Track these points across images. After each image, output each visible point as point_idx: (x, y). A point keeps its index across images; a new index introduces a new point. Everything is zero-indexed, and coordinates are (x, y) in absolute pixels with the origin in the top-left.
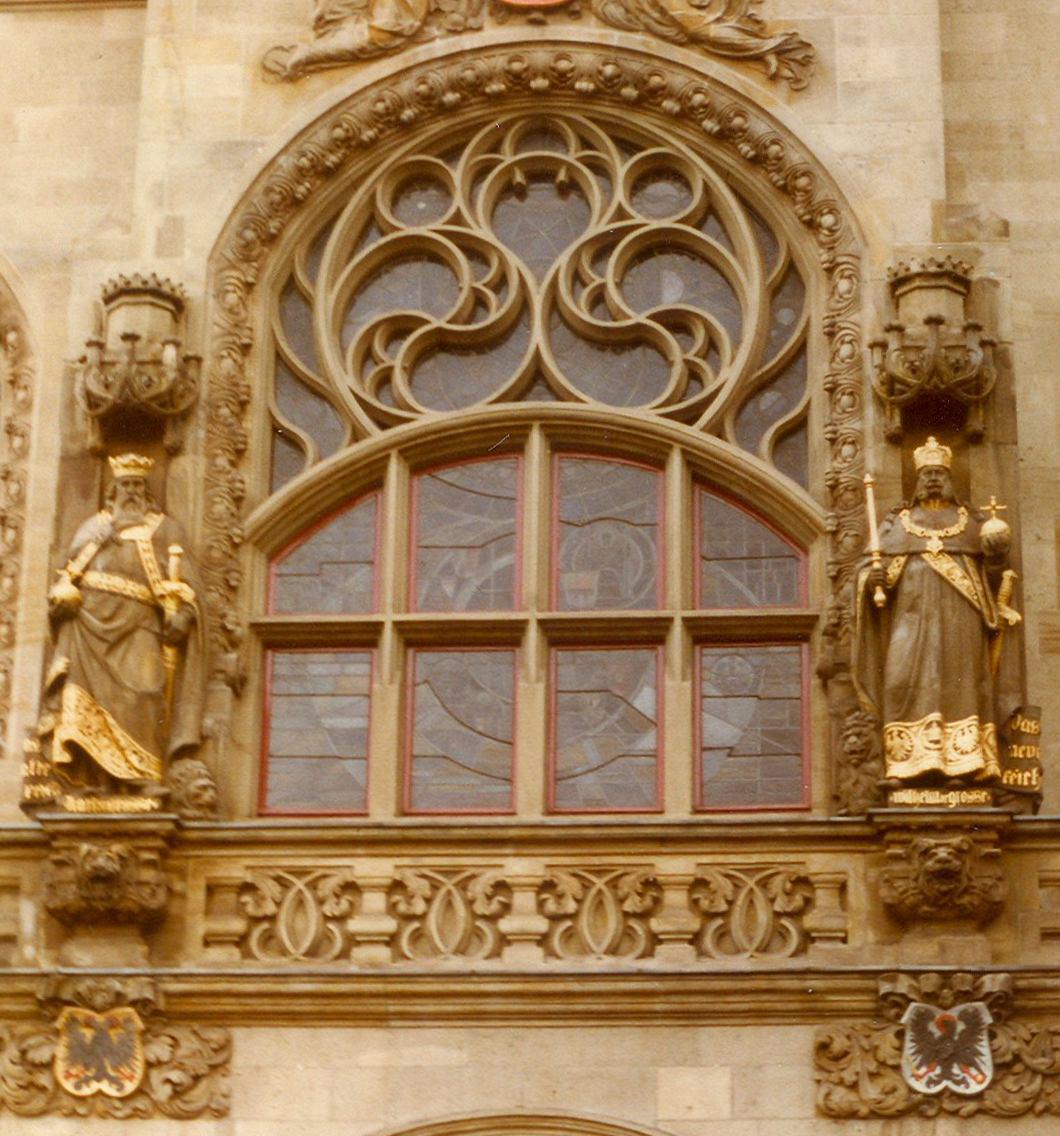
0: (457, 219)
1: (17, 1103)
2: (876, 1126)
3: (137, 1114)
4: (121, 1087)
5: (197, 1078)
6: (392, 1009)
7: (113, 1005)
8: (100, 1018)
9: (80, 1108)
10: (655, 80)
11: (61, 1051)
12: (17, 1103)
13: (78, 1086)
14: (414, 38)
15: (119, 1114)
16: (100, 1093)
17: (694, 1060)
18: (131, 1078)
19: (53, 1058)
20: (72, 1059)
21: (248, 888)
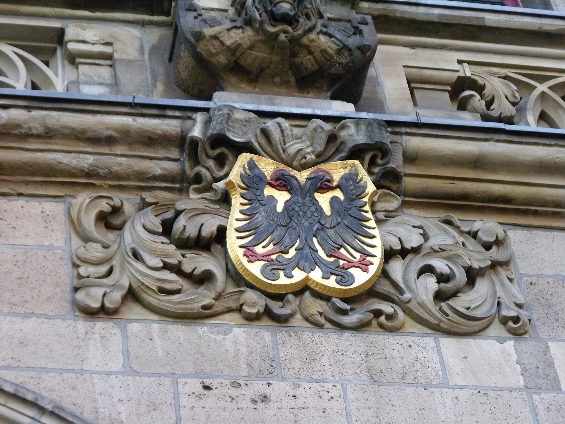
1: (162, 291)
4: (344, 277)
9: (274, 309)
12: (162, 291)
13: (273, 267)
15: (347, 320)
18: (364, 266)
19: (222, 232)
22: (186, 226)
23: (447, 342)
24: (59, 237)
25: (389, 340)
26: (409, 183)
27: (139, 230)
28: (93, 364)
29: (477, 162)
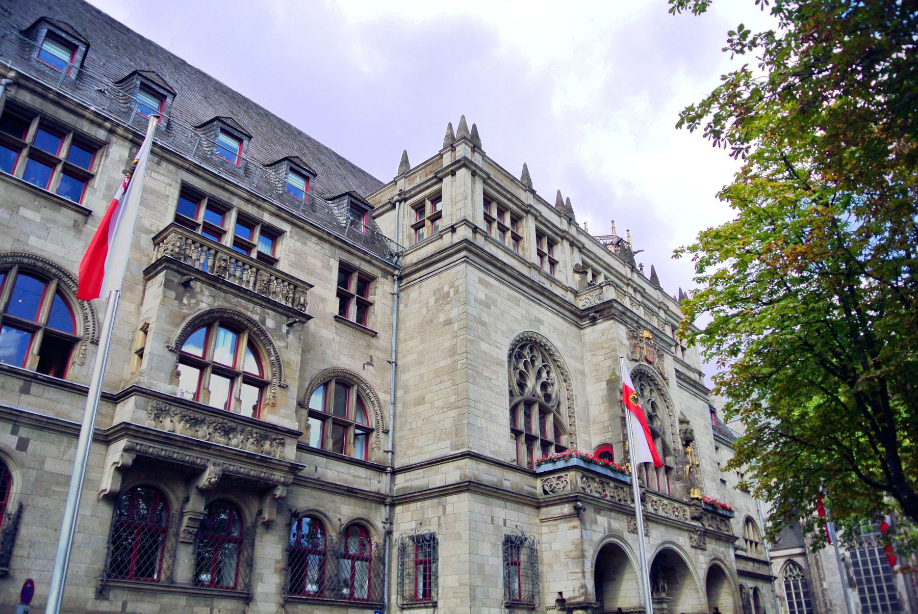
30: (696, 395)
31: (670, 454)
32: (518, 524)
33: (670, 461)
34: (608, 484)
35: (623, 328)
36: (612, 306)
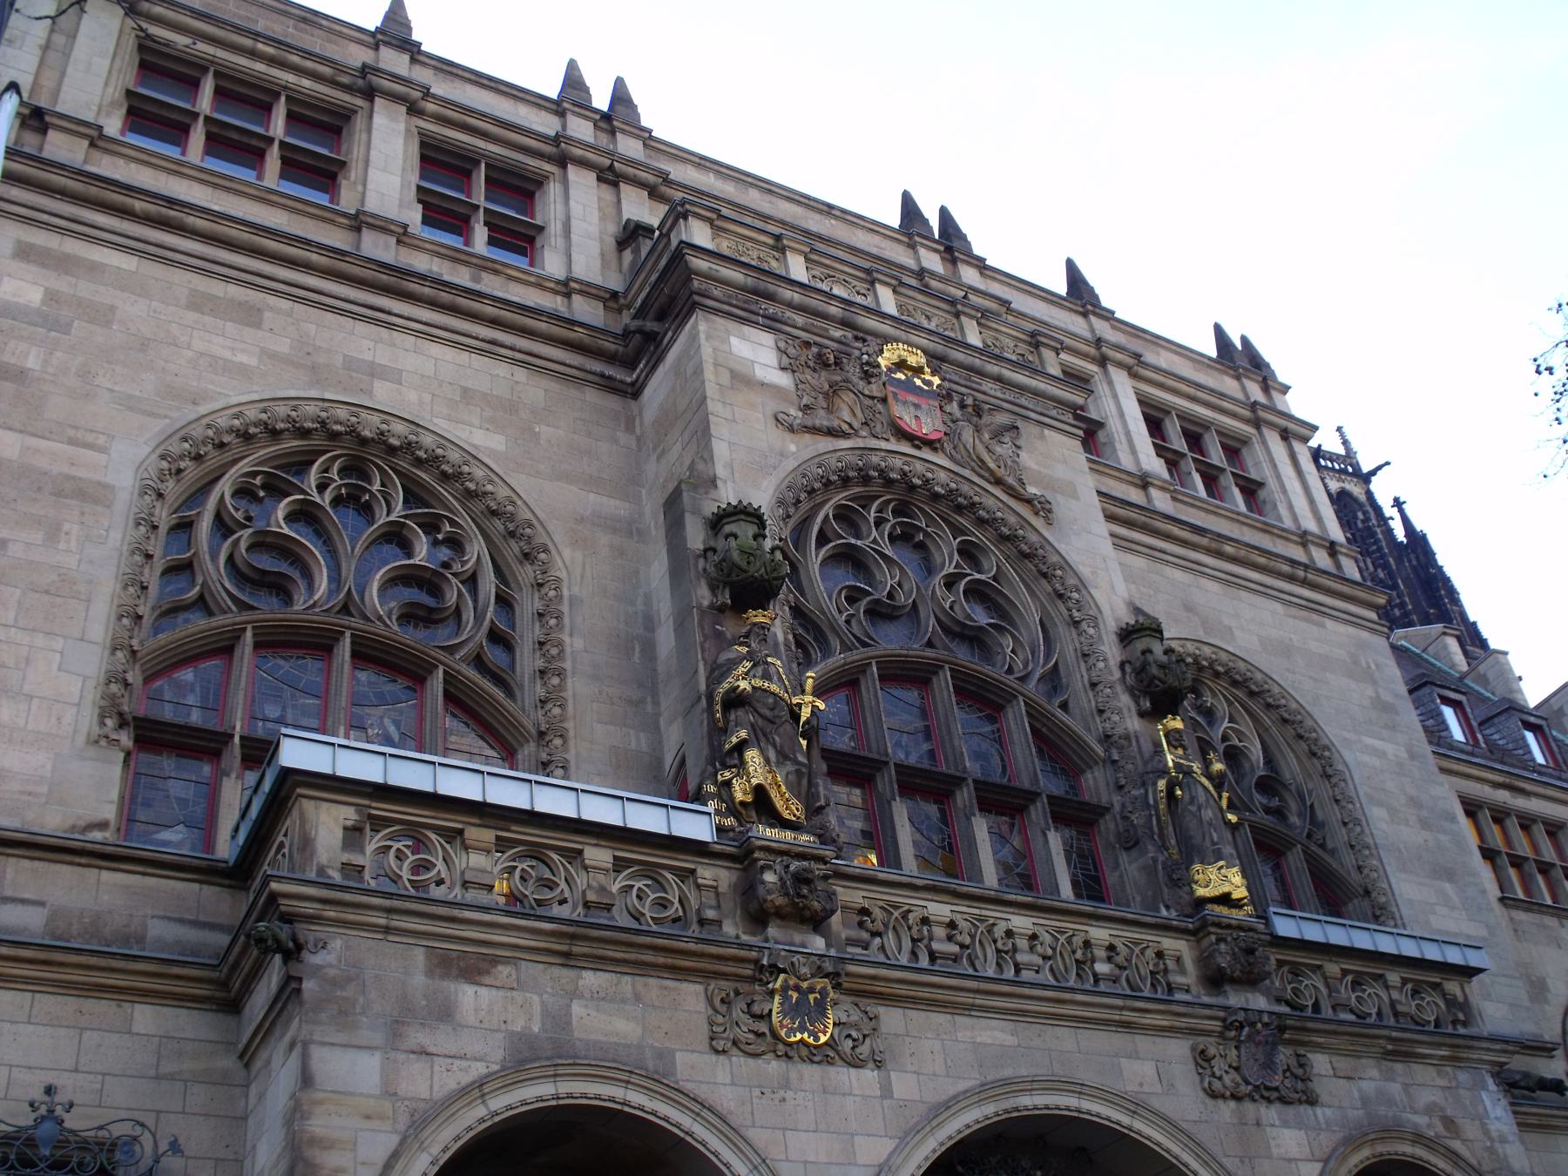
0: (875, 541)
2: (1232, 1104)
3: (828, 1061)
4: (817, 1039)
5: (865, 1036)
6: (978, 1002)
7: (813, 976)
8: (805, 985)
9: (789, 1052)
10: (976, 499)
11: (776, 1007)
14: (857, 434)
15: (817, 1059)
16: (802, 1040)
17: (1134, 1055)
18: (825, 1033)
20: (784, 1013)
21: (864, 911)
22: (756, 1009)
23: (852, 1070)
24: (701, 1006)
25: (831, 1069)
26: (845, 985)
27: (738, 1012)
28: (720, 1079)
29: (874, 978)
30: (1313, 607)
31: (1091, 761)
32: (51, 1078)
33: (1096, 784)
34: (575, 855)
35: (768, 339)
36: (690, 273)
